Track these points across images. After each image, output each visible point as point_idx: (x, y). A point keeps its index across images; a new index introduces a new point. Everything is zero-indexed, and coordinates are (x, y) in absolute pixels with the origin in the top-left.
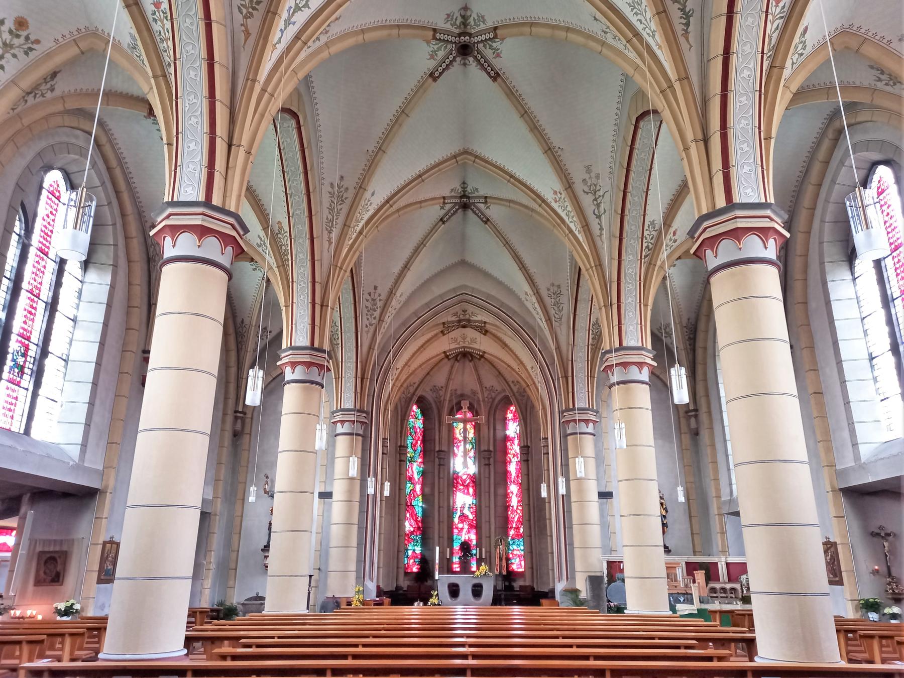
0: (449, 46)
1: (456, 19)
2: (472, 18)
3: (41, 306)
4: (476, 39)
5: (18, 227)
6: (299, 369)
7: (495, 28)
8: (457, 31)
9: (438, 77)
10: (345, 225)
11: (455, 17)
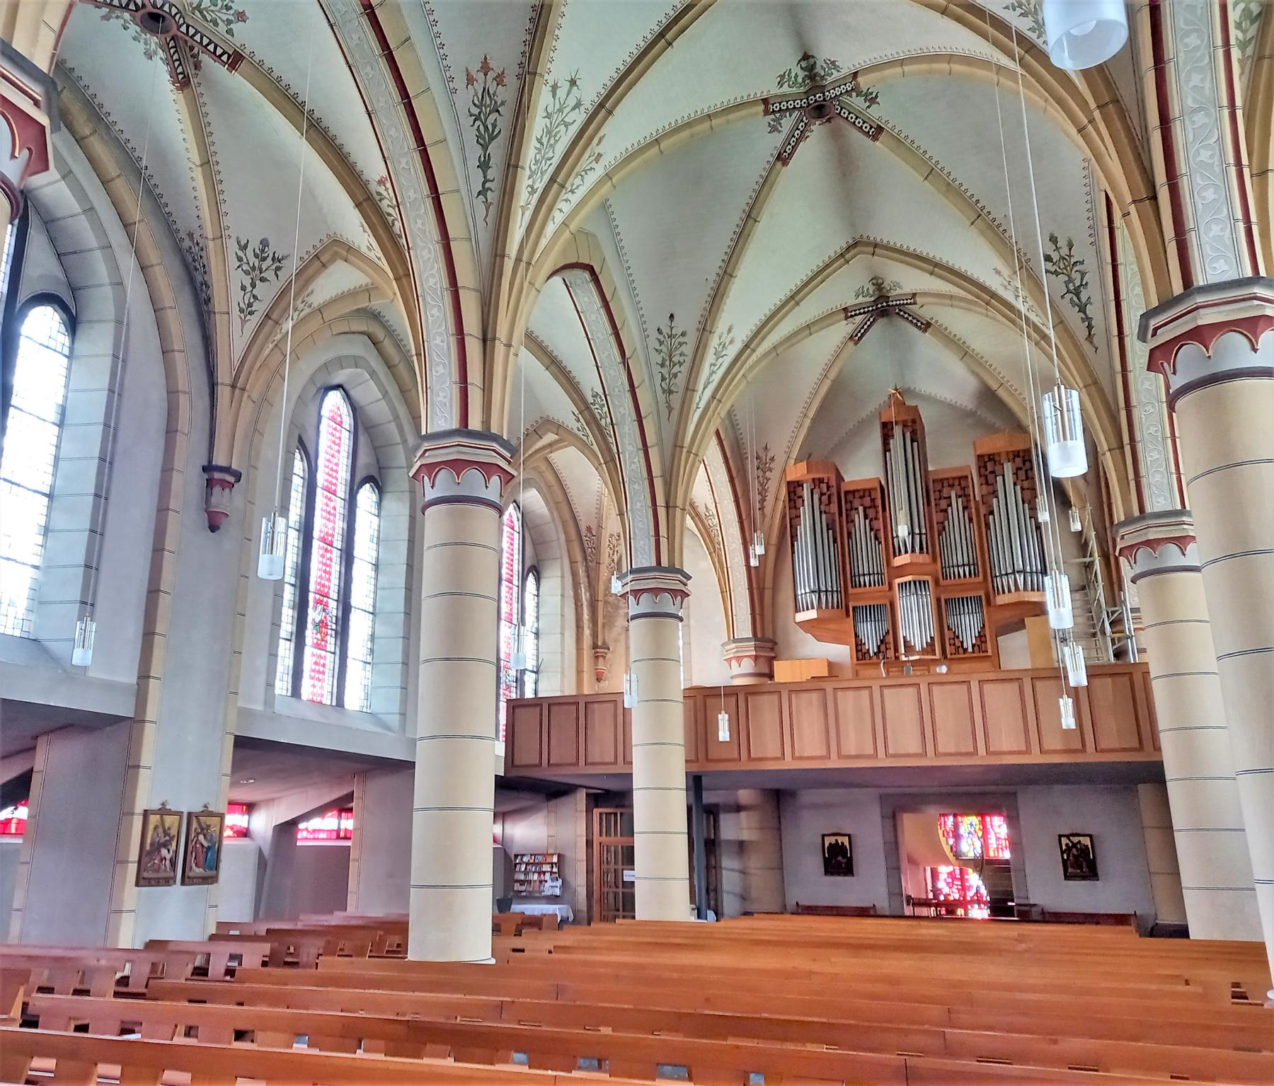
0: (796, 113)
1: (796, 75)
2: (818, 66)
3: (336, 554)
4: (833, 93)
5: (299, 466)
6: (644, 597)
7: (855, 75)
8: (802, 89)
9: (791, 155)
10: (687, 389)
11: (793, 75)
